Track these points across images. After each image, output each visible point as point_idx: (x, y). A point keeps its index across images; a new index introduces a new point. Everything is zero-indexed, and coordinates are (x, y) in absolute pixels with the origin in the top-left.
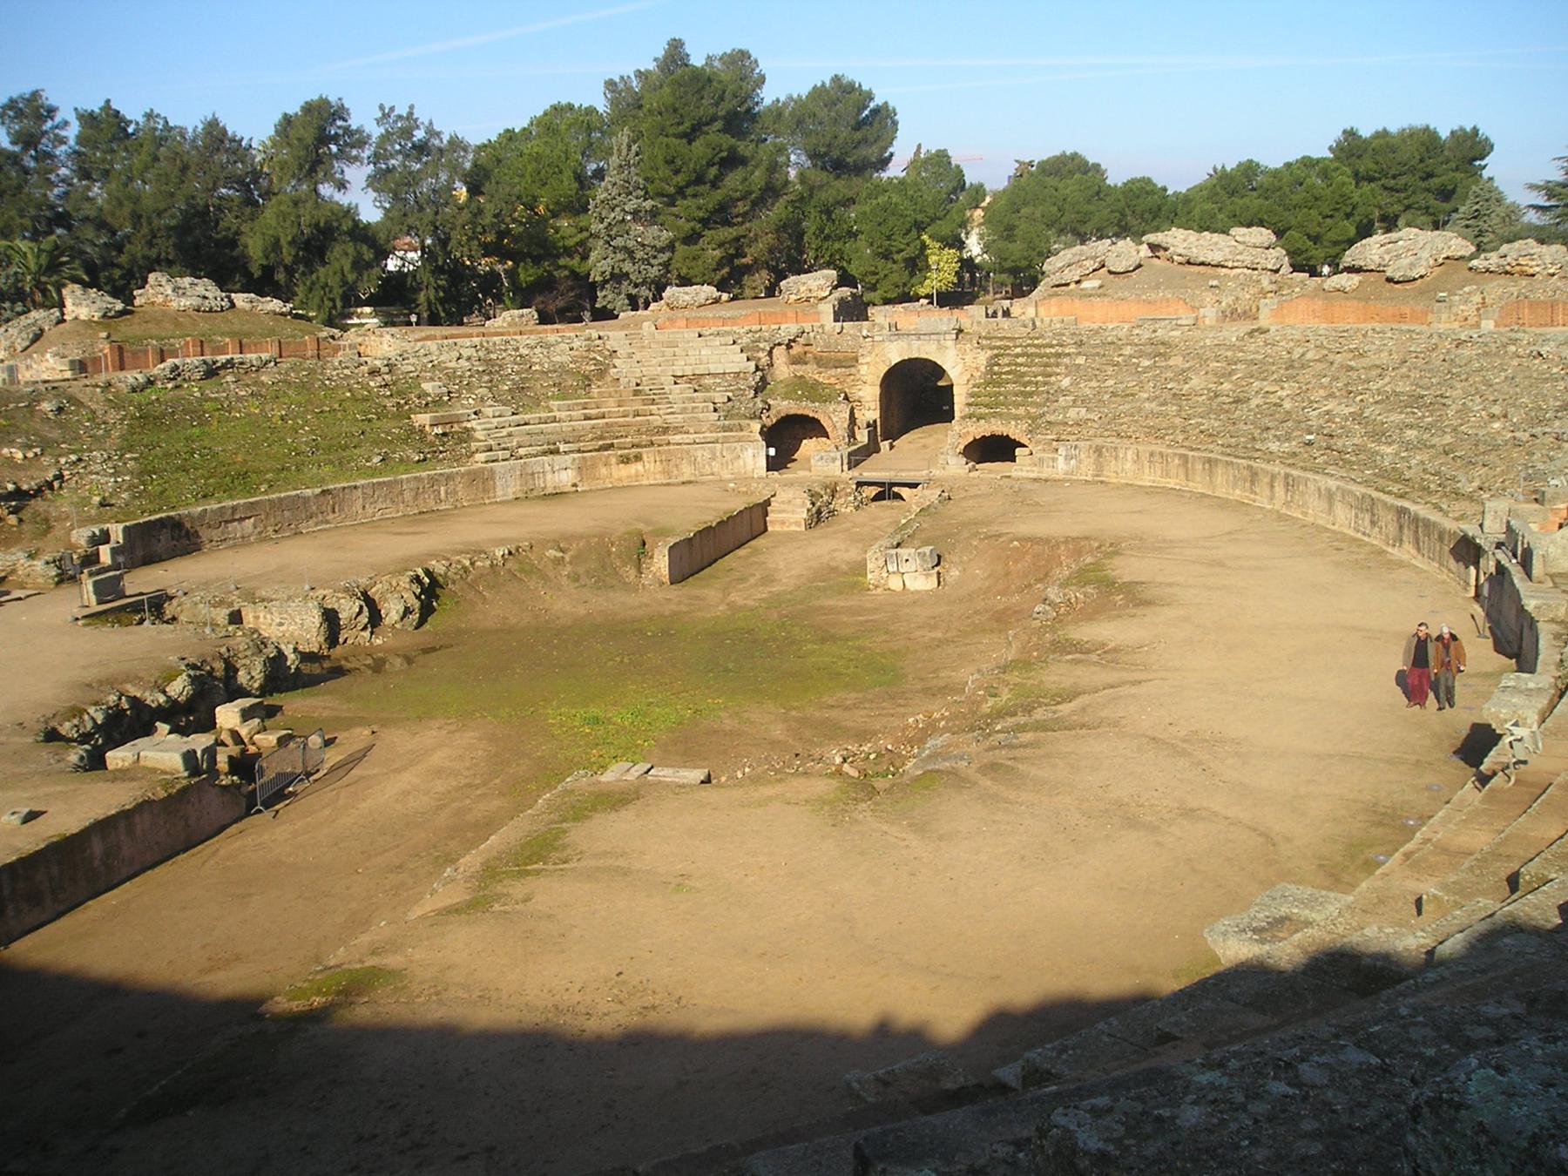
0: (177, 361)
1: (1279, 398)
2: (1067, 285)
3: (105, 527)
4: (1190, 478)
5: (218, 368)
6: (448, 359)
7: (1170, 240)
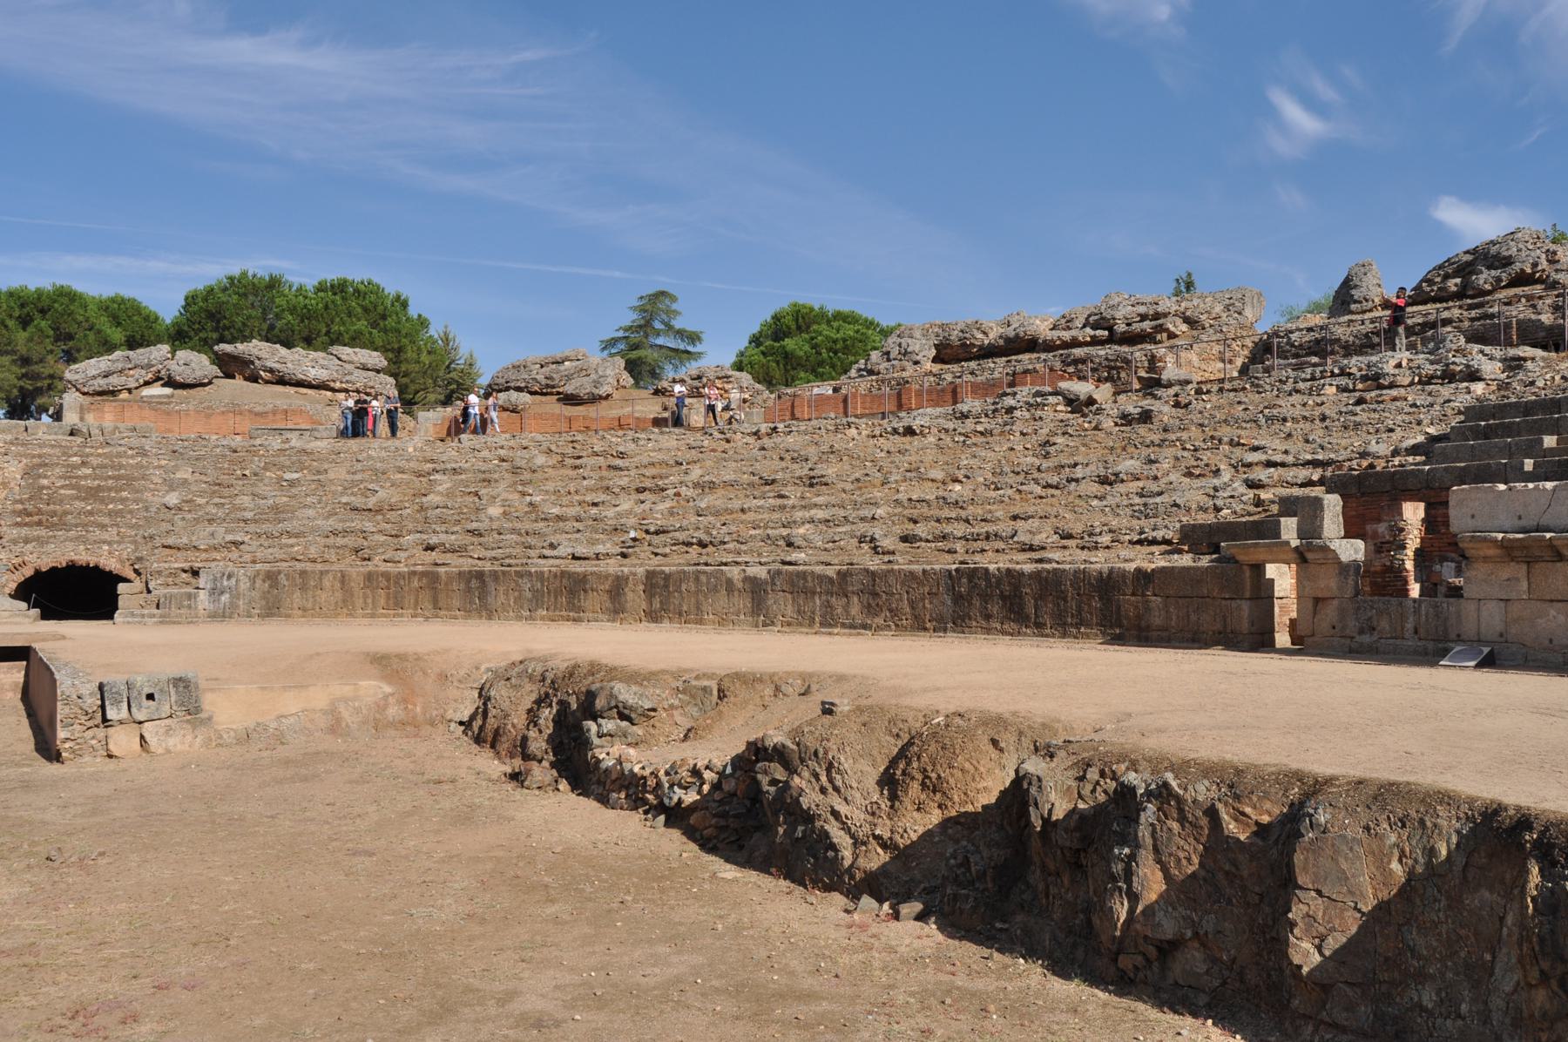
4: (440, 604)
7: (255, 352)
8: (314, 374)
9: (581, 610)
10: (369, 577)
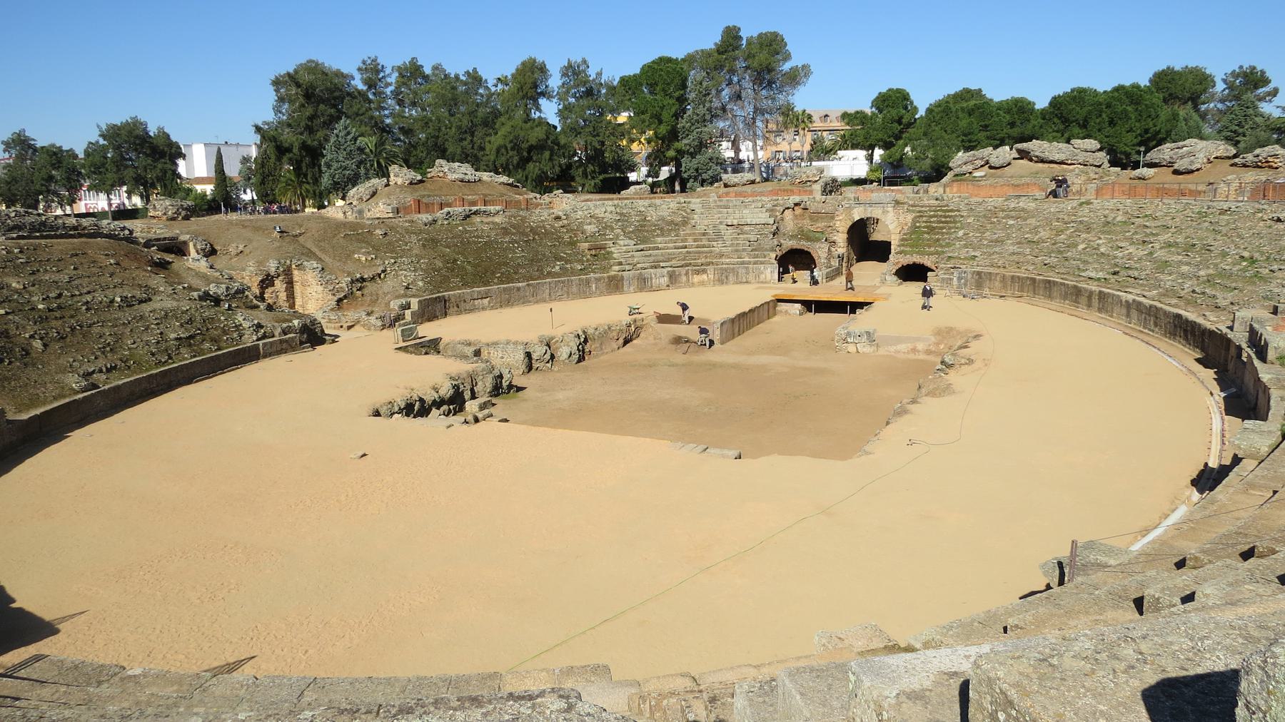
0: (449, 209)
1: (1098, 245)
2: (965, 174)
3: (409, 300)
5: (471, 214)
6: (599, 212)
8: (1057, 157)
9: (1078, 303)
10: (1013, 277)
